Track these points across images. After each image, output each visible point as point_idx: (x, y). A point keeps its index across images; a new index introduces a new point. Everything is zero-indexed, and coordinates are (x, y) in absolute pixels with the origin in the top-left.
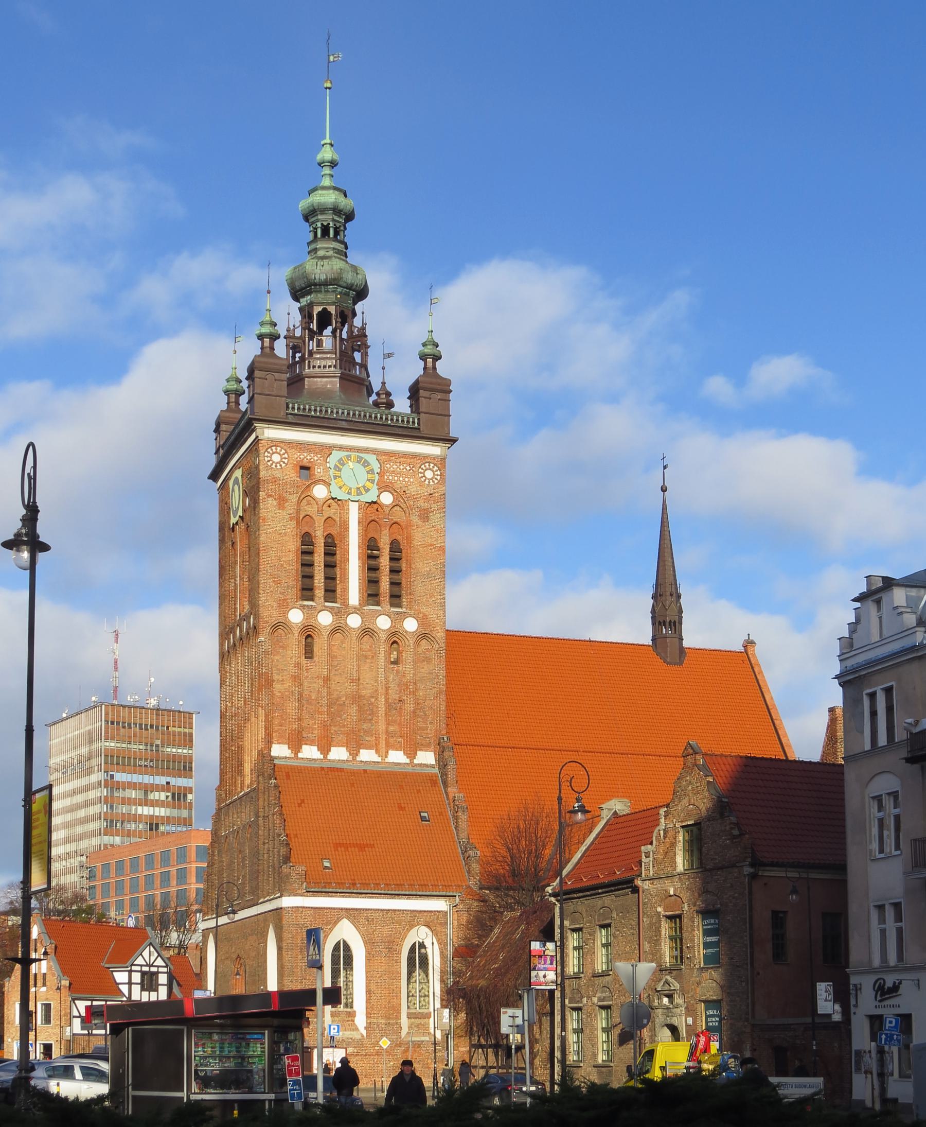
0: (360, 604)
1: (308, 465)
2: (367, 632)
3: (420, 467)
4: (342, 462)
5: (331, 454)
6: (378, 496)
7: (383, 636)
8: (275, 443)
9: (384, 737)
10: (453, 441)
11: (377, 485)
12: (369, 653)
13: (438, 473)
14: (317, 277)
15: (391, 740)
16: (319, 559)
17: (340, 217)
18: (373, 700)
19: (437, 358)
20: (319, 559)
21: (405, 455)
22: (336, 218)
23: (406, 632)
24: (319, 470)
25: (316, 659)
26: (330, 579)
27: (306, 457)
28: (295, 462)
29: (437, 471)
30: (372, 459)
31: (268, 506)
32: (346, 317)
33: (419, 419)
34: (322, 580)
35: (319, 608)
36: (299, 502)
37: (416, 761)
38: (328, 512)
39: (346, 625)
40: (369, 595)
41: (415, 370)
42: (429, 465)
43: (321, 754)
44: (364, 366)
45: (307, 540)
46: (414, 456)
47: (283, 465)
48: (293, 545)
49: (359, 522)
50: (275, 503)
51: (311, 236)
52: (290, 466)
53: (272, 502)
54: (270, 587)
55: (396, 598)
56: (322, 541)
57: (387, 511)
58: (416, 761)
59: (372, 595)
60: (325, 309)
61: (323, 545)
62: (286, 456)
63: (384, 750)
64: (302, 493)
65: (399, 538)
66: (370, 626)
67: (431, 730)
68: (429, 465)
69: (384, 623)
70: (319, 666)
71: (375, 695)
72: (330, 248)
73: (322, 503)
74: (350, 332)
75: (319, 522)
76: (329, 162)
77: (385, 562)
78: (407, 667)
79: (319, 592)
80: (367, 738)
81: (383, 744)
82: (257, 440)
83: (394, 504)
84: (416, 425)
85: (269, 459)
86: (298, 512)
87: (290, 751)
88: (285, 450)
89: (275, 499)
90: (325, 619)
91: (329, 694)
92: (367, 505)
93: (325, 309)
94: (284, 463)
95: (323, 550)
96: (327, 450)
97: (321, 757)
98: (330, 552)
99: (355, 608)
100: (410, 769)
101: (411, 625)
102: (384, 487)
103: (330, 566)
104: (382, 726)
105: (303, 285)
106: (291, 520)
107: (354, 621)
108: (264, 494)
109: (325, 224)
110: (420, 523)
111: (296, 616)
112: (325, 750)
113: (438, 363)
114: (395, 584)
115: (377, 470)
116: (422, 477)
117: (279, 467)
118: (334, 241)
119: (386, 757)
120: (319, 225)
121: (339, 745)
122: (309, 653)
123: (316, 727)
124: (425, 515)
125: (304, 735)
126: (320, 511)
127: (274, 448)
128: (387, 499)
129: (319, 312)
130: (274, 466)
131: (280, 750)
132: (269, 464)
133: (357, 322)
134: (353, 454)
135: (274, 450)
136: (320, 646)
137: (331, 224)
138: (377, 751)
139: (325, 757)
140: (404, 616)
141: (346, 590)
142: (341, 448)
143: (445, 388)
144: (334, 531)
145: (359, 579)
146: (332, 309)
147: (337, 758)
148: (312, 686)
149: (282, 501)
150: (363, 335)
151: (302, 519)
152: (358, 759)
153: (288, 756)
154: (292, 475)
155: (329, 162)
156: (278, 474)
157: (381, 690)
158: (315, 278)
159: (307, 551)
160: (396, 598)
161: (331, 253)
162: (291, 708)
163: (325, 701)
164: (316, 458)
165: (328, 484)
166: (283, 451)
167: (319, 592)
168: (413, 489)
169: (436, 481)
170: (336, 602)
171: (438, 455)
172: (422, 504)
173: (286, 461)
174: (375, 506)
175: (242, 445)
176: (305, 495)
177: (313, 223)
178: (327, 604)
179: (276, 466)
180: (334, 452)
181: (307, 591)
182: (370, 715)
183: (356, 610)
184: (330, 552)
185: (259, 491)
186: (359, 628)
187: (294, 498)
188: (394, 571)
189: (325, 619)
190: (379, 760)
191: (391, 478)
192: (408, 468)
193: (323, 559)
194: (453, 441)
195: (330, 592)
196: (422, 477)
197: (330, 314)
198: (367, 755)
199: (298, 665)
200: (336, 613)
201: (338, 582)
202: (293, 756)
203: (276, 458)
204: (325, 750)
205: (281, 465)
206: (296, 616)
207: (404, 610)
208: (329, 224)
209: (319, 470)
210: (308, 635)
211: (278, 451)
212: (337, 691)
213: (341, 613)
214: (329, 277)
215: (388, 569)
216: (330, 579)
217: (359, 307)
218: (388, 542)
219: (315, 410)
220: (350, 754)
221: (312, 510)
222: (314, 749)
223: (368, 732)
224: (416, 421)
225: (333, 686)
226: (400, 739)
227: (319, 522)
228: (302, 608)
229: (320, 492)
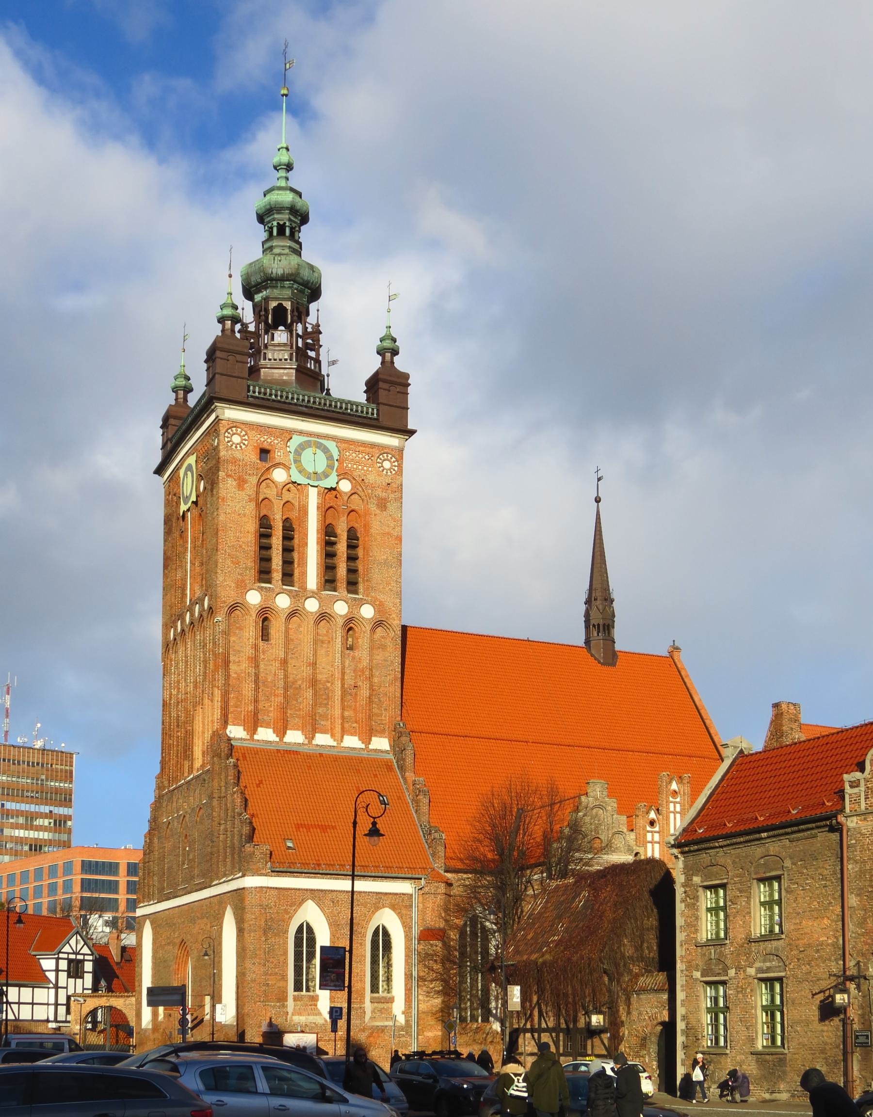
0: (317, 588)
1: (268, 447)
2: (323, 616)
3: (378, 457)
4: (302, 447)
5: (291, 438)
6: (337, 483)
7: (341, 622)
8: (235, 424)
9: (339, 722)
10: (412, 433)
11: (337, 471)
12: (325, 638)
13: (396, 464)
14: (274, 272)
15: (346, 725)
16: (277, 542)
17: (295, 217)
18: (329, 685)
19: (395, 352)
20: (277, 542)
21: (364, 444)
22: (292, 218)
23: (363, 618)
24: (279, 454)
25: (273, 641)
26: (288, 563)
27: (266, 441)
28: (255, 444)
29: (394, 462)
30: (332, 446)
31: (227, 486)
32: (301, 313)
33: (378, 410)
34: (280, 563)
35: (277, 590)
36: (259, 484)
37: (371, 747)
38: (287, 496)
39: (304, 608)
40: (327, 581)
41: (374, 364)
42: (387, 456)
43: (277, 736)
44: (317, 361)
45: (265, 524)
46: (373, 445)
47: (243, 447)
48: (251, 527)
49: (318, 508)
50: (234, 483)
51: (264, 236)
52: (250, 448)
53: (231, 483)
54: (228, 567)
55: (352, 585)
56: (281, 524)
57: (346, 498)
58: (371, 747)
59: (329, 581)
60: (280, 305)
61: (281, 528)
62: (246, 437)
63: (338, 735)
64: (262, 475)
65: (356, 525)
66: (327, 611)
67: (385, 717)
68: (387, 456)
69: (341, 608)
70: (275, 648)
71: (331, 679)
72: (286, 246)
73: (281, 487)
74: (305, 328)
75: (278, 506)
76: (285, 165)
77: (342, 548)
78: (362, 653)
79: (277, 575)
80: (322, 723)
81: (338, 728)
82: (217, 420)
83: (353, 492)
84: (375, 415)
85: (229, 439)
86: (258, 493)
87: (245, 733)
88: (246, 432)
89: (235, 479)
90: (283, 602)
91: (286, 677)
92: (326, 491)
93: (280, 305)
94: (244, 444)
95: (281, 533)
96: (288, 434)
97: (277, 739)
98: (288, 537)
99: (313, 592)
100: (365, 754)
101: (367, 612)
102: (343, 475)
103: (287, 550)
104: (337, 712)
105: (259, 280)
106: (250, 502)
107: (312, 605)
108: (224, 474)
109: (281, 223)
110: (378, 512)
111: (254, 598)
112: (281, 732)
113: (396, 358)
114: (352, 571)
115: (336, 457)
116: (379, 467)
117: (239, 448)
118: (290, 240)
119: (342, 741)
120: (275, 223)
122: (265, 635)
123: (272, 709)
124: (383, 504)
125: (260, 717)
126: (280, 495)
127: (234, 429)
128: (345, 486)
129: (274, 307)
130: (234, 447)
131: (236, 732)
132: (229, 444)
133: (311, 319)
135: (234, 431)
136: (277, 628)
137: (287, 224)
138: (333, 736)
139: (281, 740)
140: (361, 602)
141: (304, 574)
142: (301, 433)
143: (403, 381)
144: (293, 515)
145: (318, 564)
146: (288, 305)
147: (293, 741)
148: (270, 669)
149: (241, 483)
150: (317, 331)
151: (260, 502)
152: (314, 742)
153: (243, 737)
154: (253, 457)
155: (285, 165)
156: (238, 455)
157: (337, 675)
158: (272, 273)
160: (352, 585)
161: (287, 251)
162: (248, 690)
163: (281, 684)
164: (276, 441)
165: (287, 468)
166: (244, 433)
167: (277, 575)
168: (371, 478)
169: (394, 472)
170: (293, 586)
171: (396, 447)
172: (380, 493)
173: (246, 443)
174: (334, 493)
175: (197, 429)
176: (264, 479)
177: (269, 222)
178: (285, 587)
179: (236, 447)
180: (294, 437)
181: (264, 574)
182: (325, 699)
183: (314, 595)
184: (288, 537)
185: (218, 471)
186: (316, 613)
187: (254, 480)
188: (352, 558)
189: (283, 602)
190: (335, 744)
191: (350, 465)
192: (367, 457)
193: (281, 542)
194: (412, 433)
195: (288, 576)
196: (379, 467)
197: (285, 309)
198: (322, 739)
199: (256, 647)
200: (294, 596)
201: (296, 566)
202: (248, 737)
203: (236, 439)
204: (281, 732)
205: (241, 447)
206: (254, 598)
207: (361, 596)
208: (285, 223)
209: (279, 454)
210: (265, 616)
211: (238, 432)
212: (293, 674)
214: (287, 271)
215: (345, 555)
216: (288, 563)
217: (313, 307)
218: (346, 529)
219: (276, 396)
220: (306, 738)
221: (269, 492)
222: (270, 731)
223: (325, 717)
224: (375, 411)
225: (290, 669)
226: (355, 725)
227: (278, 506)
228: (260, 589)
229: (279, 475)
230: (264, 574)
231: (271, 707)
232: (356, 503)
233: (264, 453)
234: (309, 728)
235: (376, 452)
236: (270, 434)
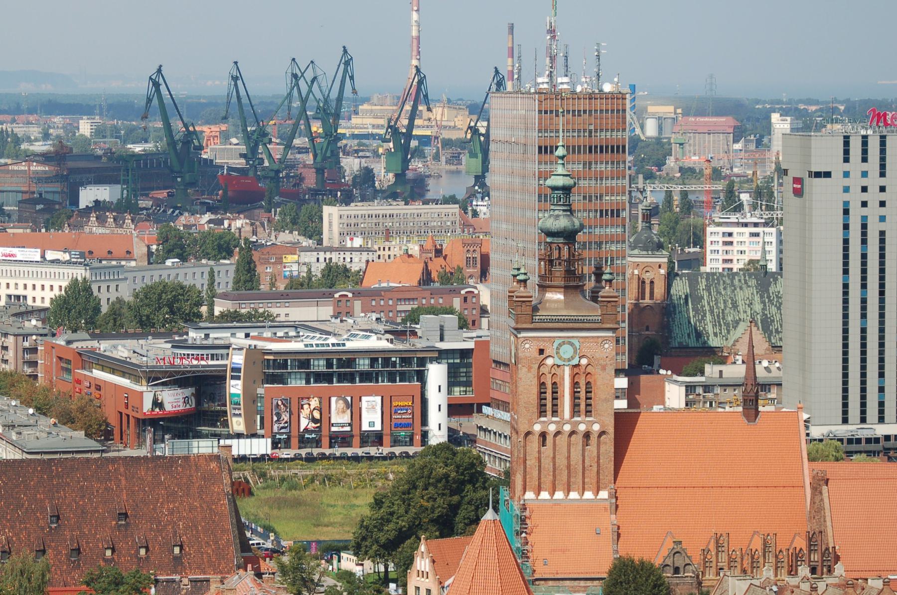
4: (561, 345)
8: (526, 339)
16: (549, 396)
20: (549, 396)
26: (554, 405)
36: (539, 367)
45: (542, 385)
48: (535, 390)
52: (534, 350)
53: (525, 370)
69: (582, 428)
79: (549, 413)
90: (552, 428)
107: (567, 428)
110: (601, 372)
112: (552, 494)
115: (578, 347)
121: (560, 490)
134: (566, 340)
136: (550, 439)
144: (557, 380)
148: (547, 463)
149: (530, 368)
154: (536, 354)
156: (528, 355)
159: (542, 394)
162: (535, 473)
167: (549, 413)
172: (602, 362)
187: (537, 366)
195: (555, 412)
203: (527, 346)
204: (552, 494)
206: (537, 428)
210: (543, 435)
213: (560, 424)
216: (554, 405)
223: (575, 483)
230: (542, 412)
231: (547, 480)
232: (589, 369)
233: (541, 351)
234: (566, 491)
235: (600, 340)
236: (544, 341)
